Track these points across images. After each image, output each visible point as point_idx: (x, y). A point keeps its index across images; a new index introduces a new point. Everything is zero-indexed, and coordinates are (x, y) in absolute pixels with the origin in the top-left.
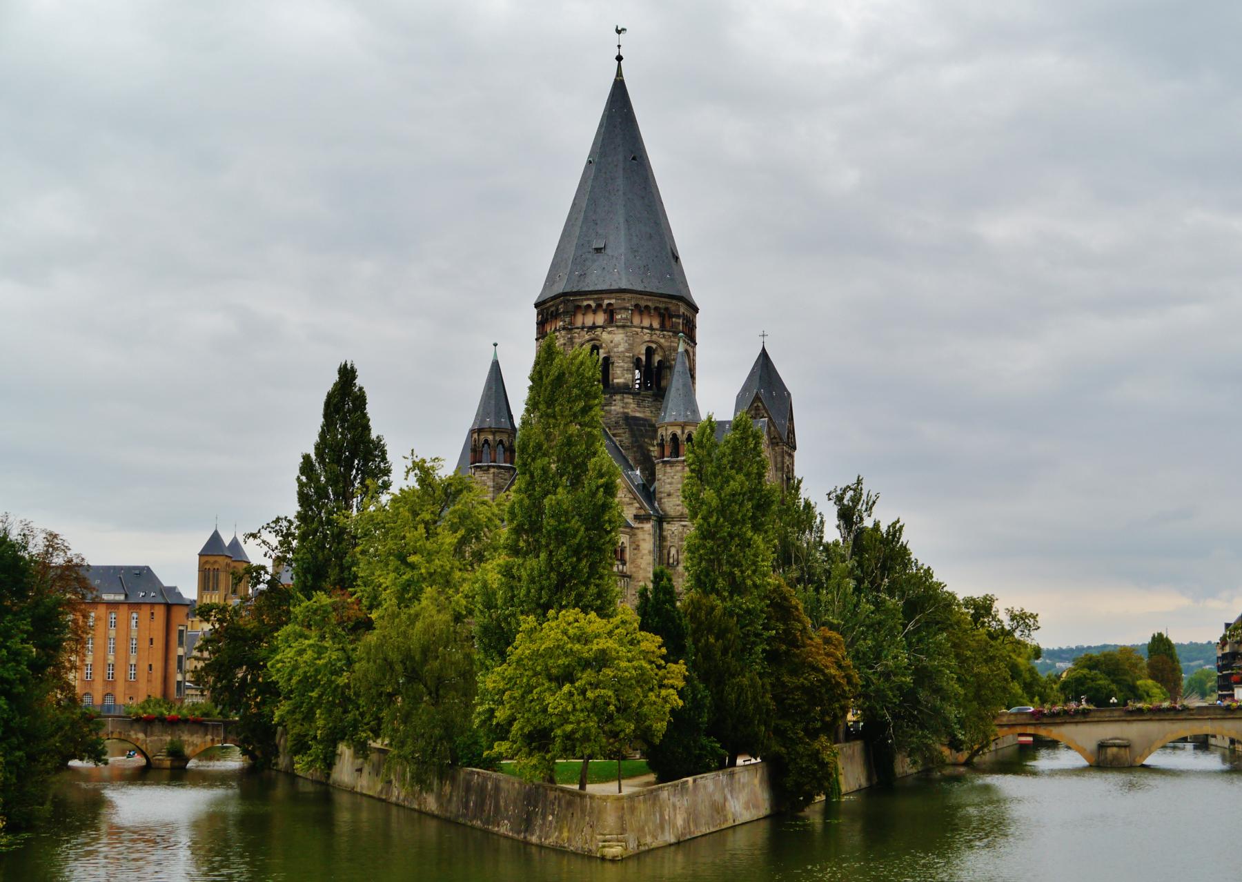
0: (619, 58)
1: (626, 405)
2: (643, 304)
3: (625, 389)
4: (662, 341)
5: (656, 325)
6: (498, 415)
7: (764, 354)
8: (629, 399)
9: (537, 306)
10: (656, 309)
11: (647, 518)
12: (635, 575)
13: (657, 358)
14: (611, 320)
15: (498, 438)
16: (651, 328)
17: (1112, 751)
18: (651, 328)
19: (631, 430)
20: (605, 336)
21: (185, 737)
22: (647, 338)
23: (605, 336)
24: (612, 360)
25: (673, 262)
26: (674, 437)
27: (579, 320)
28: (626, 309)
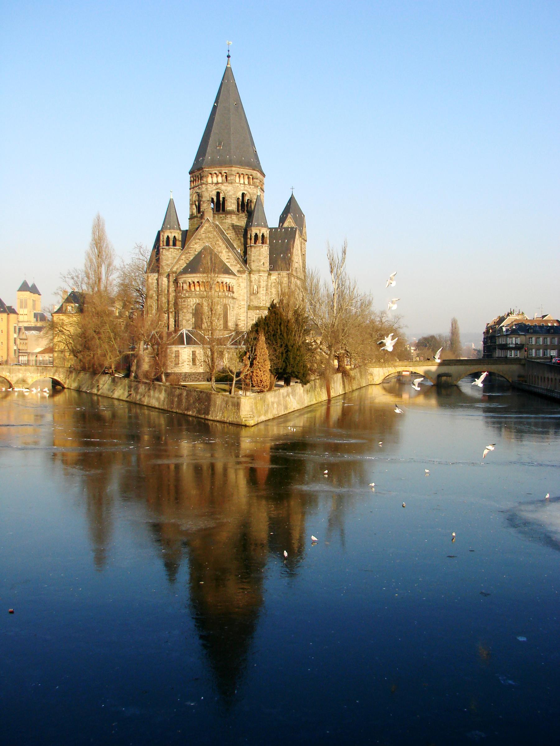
1: (232, 220)
2: (240, 173)
3: (231, 213)
4: (249, 190)
5: (246, 182)
8: (234, 217)
9: (190, 173)
11: (244, 272)
12: (238, 298)
13: (246, 198)
15: (173, 235)
19: (235, 232)
21: (28, 374)
22: (242, 188)
23: (223, 187)
24: (226, 199)
26: (256, 234)
27: (210, 180)
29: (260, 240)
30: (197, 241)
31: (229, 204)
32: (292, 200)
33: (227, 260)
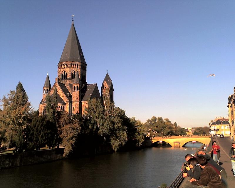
3: (69, 79)
7: (107, 75)
8: (70, 81)
15: (47, 89)
26: (75, 86)
29: (76, 89)
31: (68, 76)
32: (107, 75)
33: (63, 97)
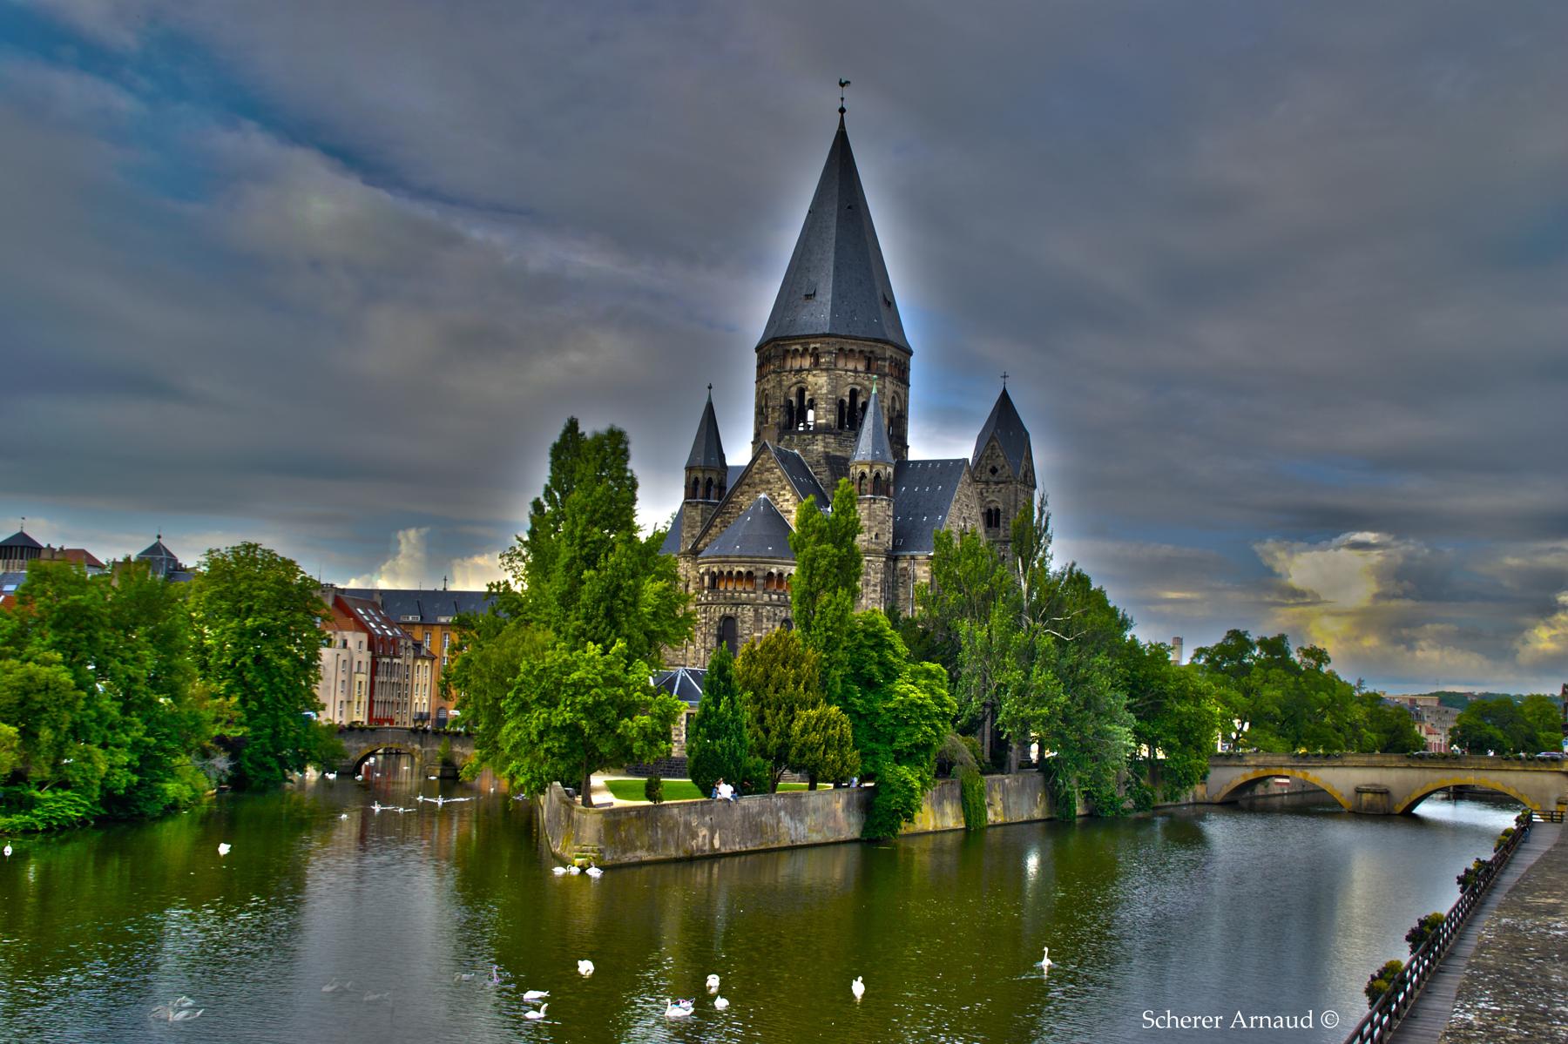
0: (842, 110)
2: (847, 347)
5: (861, 367)
6: (707, 454)
7: (1005, 396)
10: (861, 352)
13: (861, 400)
14: (816, 364)
16: (855, 371)
17: (1366, 797)
18: (855, 371)
19: (831, 470)
20: (810, 378)
21: (457, 749)
23: (810, 378)
25: (883, 308)
26: (863, 475)
28: (830, 353)
30: (745, 488)
